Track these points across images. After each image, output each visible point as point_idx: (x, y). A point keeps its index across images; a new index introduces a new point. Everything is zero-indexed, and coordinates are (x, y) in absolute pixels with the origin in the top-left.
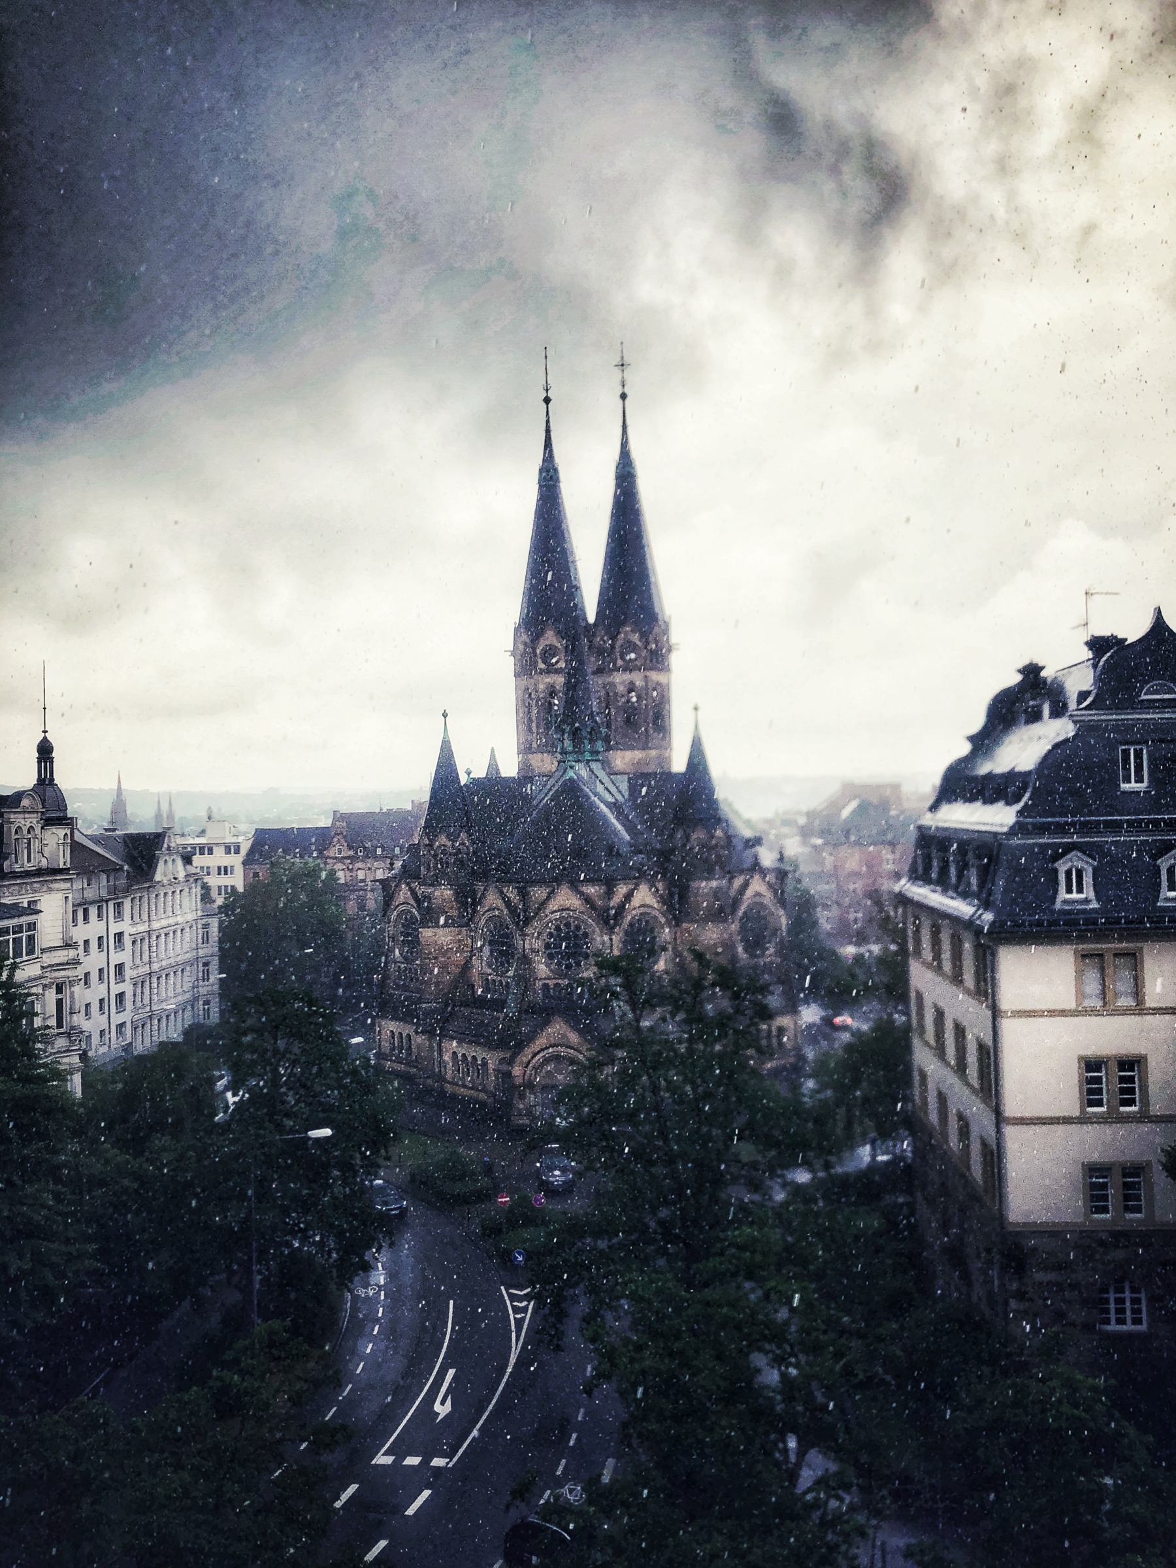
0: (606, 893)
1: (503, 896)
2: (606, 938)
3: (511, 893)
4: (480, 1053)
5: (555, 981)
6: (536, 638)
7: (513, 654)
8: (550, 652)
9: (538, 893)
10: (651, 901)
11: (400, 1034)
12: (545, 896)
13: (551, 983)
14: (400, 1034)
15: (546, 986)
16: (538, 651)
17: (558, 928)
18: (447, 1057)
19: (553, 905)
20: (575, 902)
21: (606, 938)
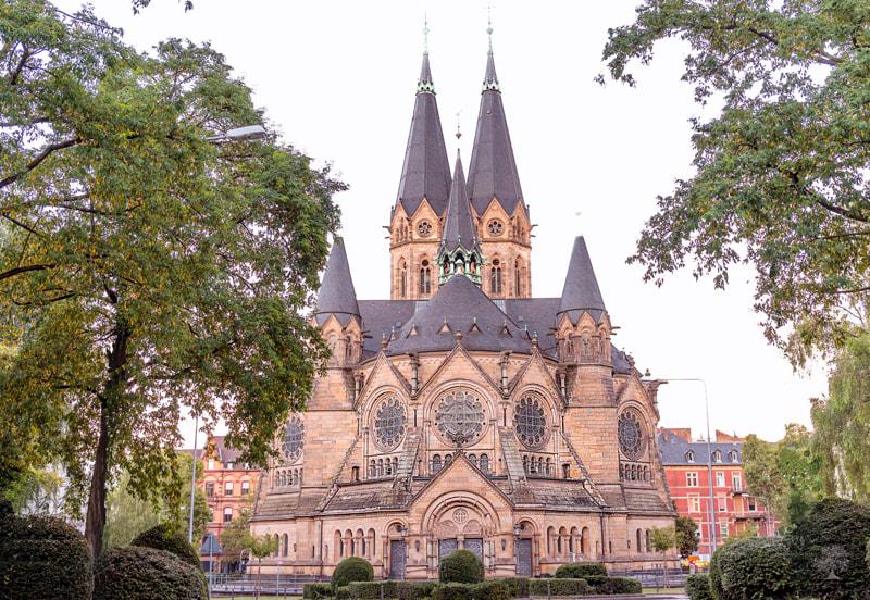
0: (500, 364)
1: (394, 369)
3: (404, 366)
4: (366, 524)
5: (446, 453)
6: (410, 215)
7: (390, 229)
8: (424, 227)
9: (431, 363)
12: (438, 364)
13: (442, 454)
16: (414, 224)
18: (329, 539)
19: (445, 376)
21: (501, 406)
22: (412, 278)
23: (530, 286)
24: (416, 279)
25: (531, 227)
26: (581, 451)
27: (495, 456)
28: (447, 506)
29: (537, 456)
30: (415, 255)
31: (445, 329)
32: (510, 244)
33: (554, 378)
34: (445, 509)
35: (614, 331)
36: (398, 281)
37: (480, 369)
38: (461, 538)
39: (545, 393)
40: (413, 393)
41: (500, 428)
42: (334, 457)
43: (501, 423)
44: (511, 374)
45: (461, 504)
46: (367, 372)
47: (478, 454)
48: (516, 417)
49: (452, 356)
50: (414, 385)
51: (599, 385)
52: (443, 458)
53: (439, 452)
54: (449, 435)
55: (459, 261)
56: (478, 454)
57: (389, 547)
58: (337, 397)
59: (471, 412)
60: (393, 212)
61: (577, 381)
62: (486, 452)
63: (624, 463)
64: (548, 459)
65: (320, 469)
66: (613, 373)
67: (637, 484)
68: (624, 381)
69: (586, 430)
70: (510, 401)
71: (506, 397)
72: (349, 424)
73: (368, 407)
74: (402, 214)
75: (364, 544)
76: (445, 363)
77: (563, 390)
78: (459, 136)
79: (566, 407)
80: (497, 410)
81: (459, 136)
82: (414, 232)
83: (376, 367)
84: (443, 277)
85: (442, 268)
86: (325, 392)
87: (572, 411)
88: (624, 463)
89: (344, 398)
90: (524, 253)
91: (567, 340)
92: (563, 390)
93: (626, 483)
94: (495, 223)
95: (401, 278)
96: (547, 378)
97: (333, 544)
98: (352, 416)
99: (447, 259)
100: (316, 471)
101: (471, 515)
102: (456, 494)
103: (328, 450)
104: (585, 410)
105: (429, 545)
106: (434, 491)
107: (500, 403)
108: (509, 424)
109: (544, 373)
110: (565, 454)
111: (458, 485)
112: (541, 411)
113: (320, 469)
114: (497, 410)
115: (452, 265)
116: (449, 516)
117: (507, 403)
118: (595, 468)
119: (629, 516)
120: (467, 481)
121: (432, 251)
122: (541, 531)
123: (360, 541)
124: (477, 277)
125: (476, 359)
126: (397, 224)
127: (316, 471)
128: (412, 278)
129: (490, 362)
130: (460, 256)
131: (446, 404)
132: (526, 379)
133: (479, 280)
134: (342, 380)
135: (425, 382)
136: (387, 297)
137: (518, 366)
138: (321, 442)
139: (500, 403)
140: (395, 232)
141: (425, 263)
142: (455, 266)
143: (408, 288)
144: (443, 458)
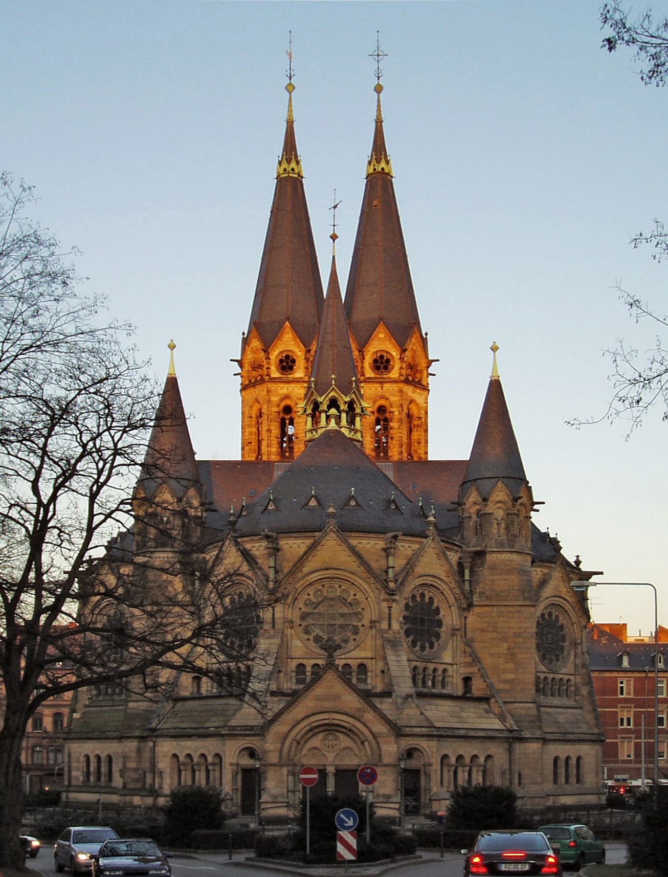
0: (385, 550)
1: (246, 555)
2: (385, 605)
3: (258, 548)
7: (240, 363)
9: (294, 546)
10: (440, 570)
11: (98, 758)
12: (303, 549)
14: (98, 758)
15: (301, 666)
16: (275, 355)
18: (164, 764)
20: (345, 558)
21: (385, 605)
22: (269, 431)
23: (427, 442)
24: (276, 431)
25: (430, 363)
26: (487, 661)
27: (374, 667)
28: (313, 731)
29: (431, 666)
30: (275, 399)
31: (313, 503)
32: (401, 385)
33: (455, 567)
34: (310, 734)
35: (536, 507)
36: (251, 434)
37: (358, 555)
38: (331, 770)
39: (443, 587)
41: (382, 632)
43: (384, 626)
44: (397, 562)
45: (331, 728)
46: (210, 555)
47: (354, 663)
48: (405, 617)
49: (322, 537)
50: (272, 575)
51: (513, 577)
52: (309, 668)
53: (304, 661)
54: (317, 639)
55: (333, 411)
56: (354, 663)
57: (240, 777)
59: (346, 611)
60: (246, 342)
61: (486, 571)
62: (365, 661)
63: (542, 676)
64: (445, 670)
66: (533, 562)
67: (556, 701)
68: (546, 571)
69: (495, 635)
70: (397, 597)
71: (391, 593)
74: (256, 344)
75: (208, 771)
76: (312, 548)
77: (467, 584)
78: (334, 237)
79: (470, 606)
80: (380, 610)
81: (334, 237)
82: (273, 368)
83: (220, 551)
84: (311, 431)
85: (309, 419)
87: (477, 610)
88: (542, 676)
90: (418, 396)
91: (474, 516)
92: (467, 586)
93: (542, 699)
94: (382, 357)
95: (254, 430)
96: (446, 567)
97: (168, 770)
99: (316, 406)
101: (344, 741)
102: (326, 716)
104: (495, 609)
105: (290, 777)
106: (299, 711)
107: (383, 600)
108: (396, 626)
109: (443, 562)
110: (470, 665)
111: (327, 705)
112: (437, 611)
114: (380, 610)
115: (323, 416)
116: (316, 741)
117: (394, 600)
118: (505, 682)
119: (545, 741)
121: (298, 391)
122: (433, 760)
123: (203, 768)
124: (356, 431)
125: (354, 542)
126: (250, 356)
128: (269, 431)
129: (370, 545)
130: (333, 403)
132: (419, 569)
133: (358, 436)
135: (286, 571)
136: (240, 459)
137: (409, 552)
139: (383, 600)
140: (247, 367)
141: (288, 410)
142: (328, 417)
143: (264, 444)
144: (309, 668)
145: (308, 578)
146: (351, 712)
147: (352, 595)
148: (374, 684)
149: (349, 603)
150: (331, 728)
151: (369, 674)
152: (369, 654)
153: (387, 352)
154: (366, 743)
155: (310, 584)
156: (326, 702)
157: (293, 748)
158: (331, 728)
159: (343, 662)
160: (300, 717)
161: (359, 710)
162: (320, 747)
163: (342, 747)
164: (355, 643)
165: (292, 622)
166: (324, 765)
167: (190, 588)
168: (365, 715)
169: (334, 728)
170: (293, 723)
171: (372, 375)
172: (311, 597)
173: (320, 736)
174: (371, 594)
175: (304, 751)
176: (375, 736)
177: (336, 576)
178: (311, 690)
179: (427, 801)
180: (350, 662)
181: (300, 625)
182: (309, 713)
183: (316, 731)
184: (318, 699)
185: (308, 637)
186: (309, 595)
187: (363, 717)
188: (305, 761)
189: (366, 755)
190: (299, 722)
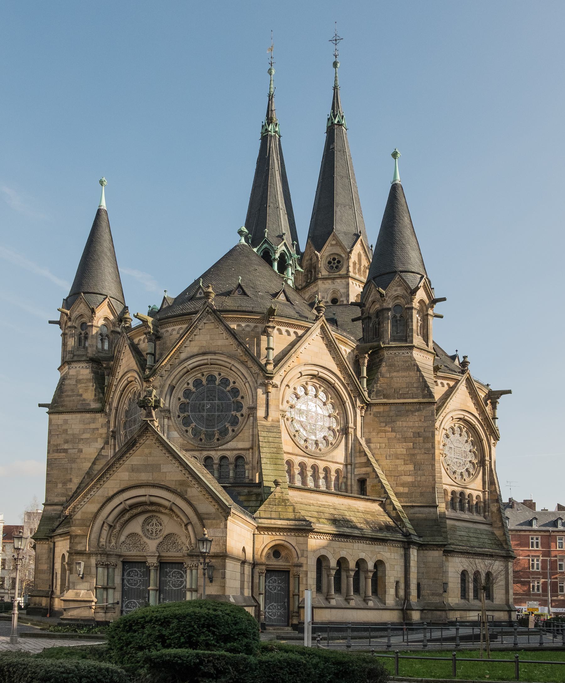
17: (198, 383)
40: (147, 372)
42: (79, 469)
54: (196, 433)
58: (85, 396)
62: (242, 453)
65: (64, 484)
72: (97, 429)
73: (115, 404)
86: (73, 390)
89: (93, 397)
98: (101, 419)
100: (60, 485)
103: (73, 460)
111: (144, 477)
113: (64, 484)
116: (136, 526)
120: (160, 470)
127: (60, 485)
131: (193, 389)
134: (91, 376)
138: (65, 451)
145: (186, 365)
146: (172, 486)
147: (231, 382)
148: (250, 478)
149: (229, 391)
150: (150, 508)
151: (247, 467)
152: (247, 445)
153: (338, 254)
154: (190, 527)
155: (188, 371)
156: (143, 474)
157: (105, 533)
158: (150, 508)
159: (220, 453)
160: (111, 493)
161: (182, 483)
162: (141, 533)
163: (166, 533)
164: (234, 433)
165: (169, 411)
166: (145, 556)
167: (101, 395)
168: (189, 490)
169: (154, 508)
170: (105, 499)
171: (327, 273)
172: (191, 387)
173: (141, 519)
174: (249, 379)
175: (123, 538)
176: (201, 518)
177: (213, 361)
178: (125, 458)
179: (296, 609)
180: (228, 454)
181: (179, 416)
182: (122, 487)
183: (135, 511)
184: (134, 469)
185: (186, 428)
186: (188, 384)
187: (186, 491)
188: (125, 551)
189: (190, 543)
190: (110, 499)
